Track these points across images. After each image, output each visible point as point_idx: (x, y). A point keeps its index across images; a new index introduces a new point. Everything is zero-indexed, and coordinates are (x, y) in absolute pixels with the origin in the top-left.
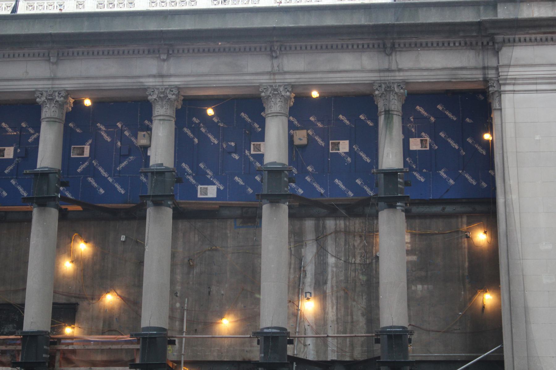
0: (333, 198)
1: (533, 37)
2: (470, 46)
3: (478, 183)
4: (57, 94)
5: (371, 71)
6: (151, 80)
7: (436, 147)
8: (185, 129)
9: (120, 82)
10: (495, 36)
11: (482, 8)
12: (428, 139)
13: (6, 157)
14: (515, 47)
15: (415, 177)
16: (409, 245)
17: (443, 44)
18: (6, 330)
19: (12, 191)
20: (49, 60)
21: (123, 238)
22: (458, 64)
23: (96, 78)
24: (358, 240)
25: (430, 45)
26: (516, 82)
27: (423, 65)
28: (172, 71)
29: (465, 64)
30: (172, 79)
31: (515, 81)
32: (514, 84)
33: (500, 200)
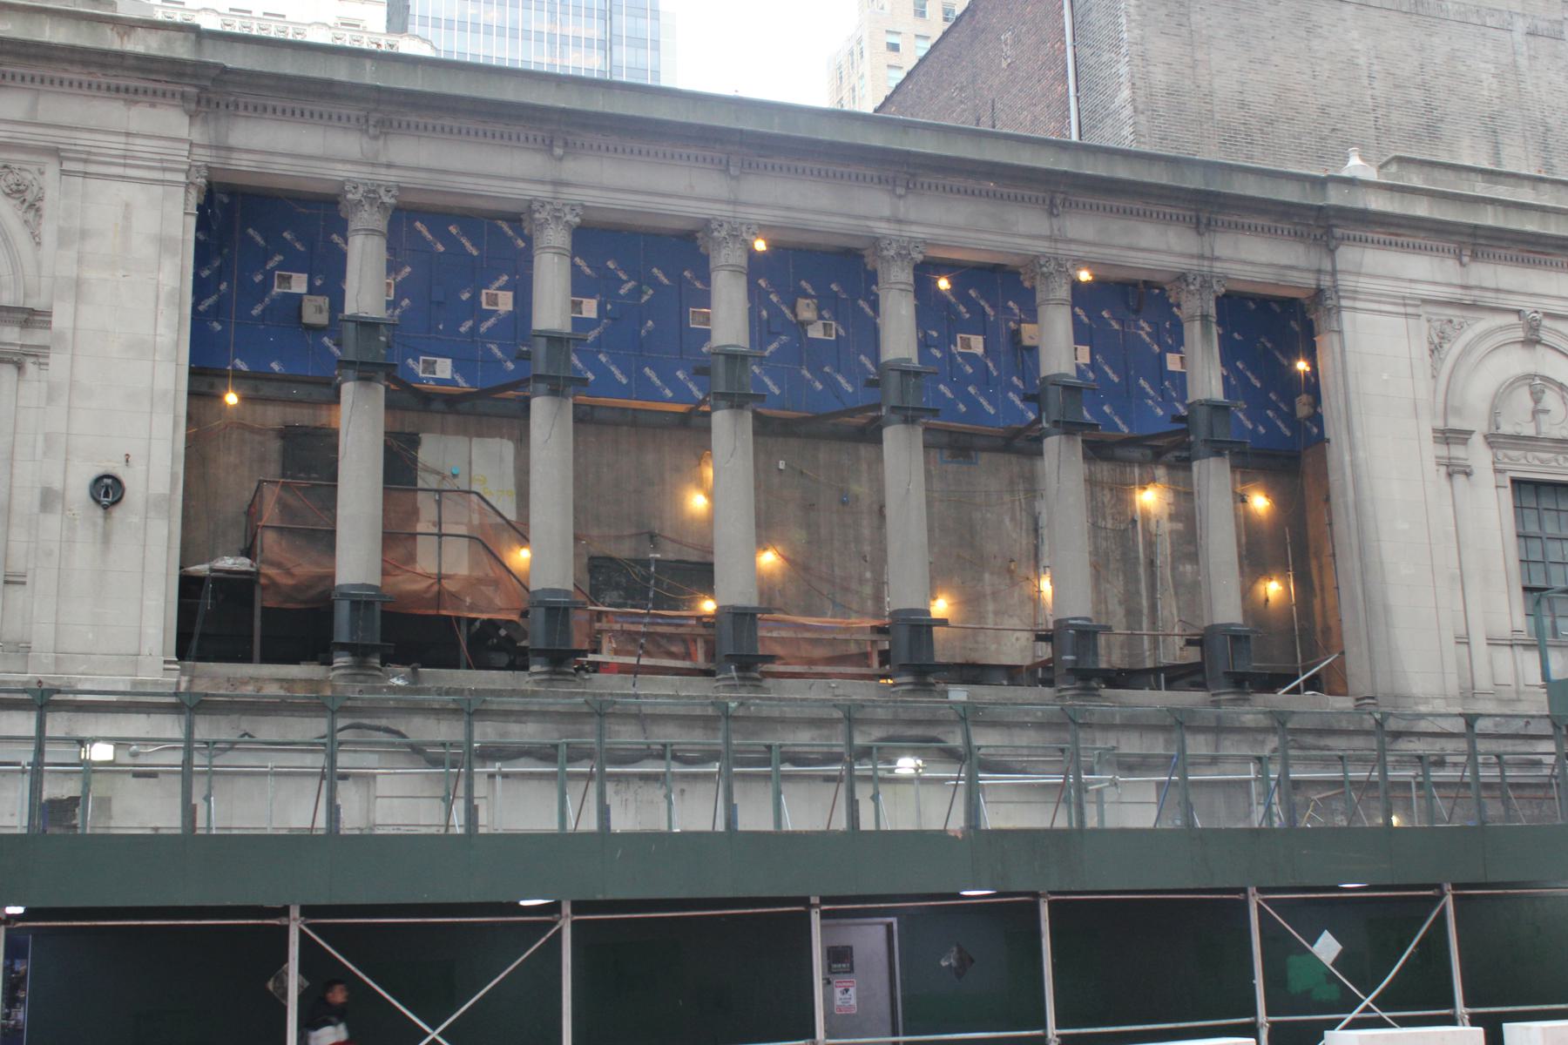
0: (1132, 432)
2: (1297, 236)
3: (1255, 427)
4: (744, 228)
5: (1182, 255)
6: (883, 225)
8: (861, 302)
9: (837, 223)
11: (1308, 186)
13: (585, 315)
18: (608, 600)
19: (602, 371)
20: (893, 191)
21: (782, 465)
22: (1284, 261)
23: (804, 210)
24: (1106, 492)
27: (1243, 256)
28: (912, 216)
30: (914, 228)
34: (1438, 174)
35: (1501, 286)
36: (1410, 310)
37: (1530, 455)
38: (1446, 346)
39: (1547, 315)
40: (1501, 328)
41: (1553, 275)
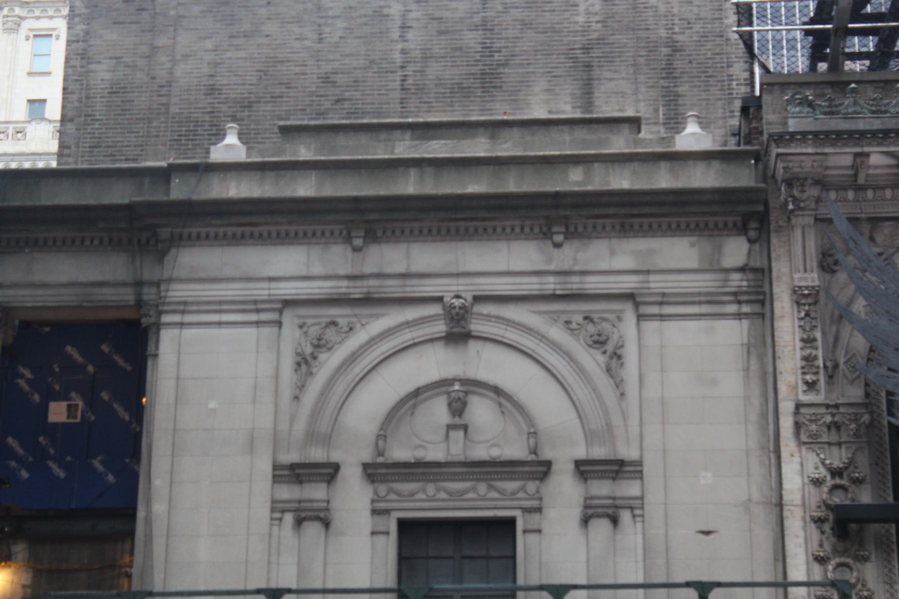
1: (221, 231)
2: (116, 245)
7: (93, 418)
10: (158, 230)
11: (147, 180)
12: (81, 404)
14: (181, 249)
15: (50, 469)
16: (29, 591)
17: (73, 242)
22: (94, 275)
25: (50, 243)
26: (187, 308)
27: (37, 277)
29: (108, 277)
31: (184, 307)
32: (183, 312)
33: (141, 514)
34: (342, 140)
35: (415, 268)
36: (264, 317)
37: (431, 488)
38: (322, 357)
39: (477, 299)
40: (408, 324)
41: (503, 245)
